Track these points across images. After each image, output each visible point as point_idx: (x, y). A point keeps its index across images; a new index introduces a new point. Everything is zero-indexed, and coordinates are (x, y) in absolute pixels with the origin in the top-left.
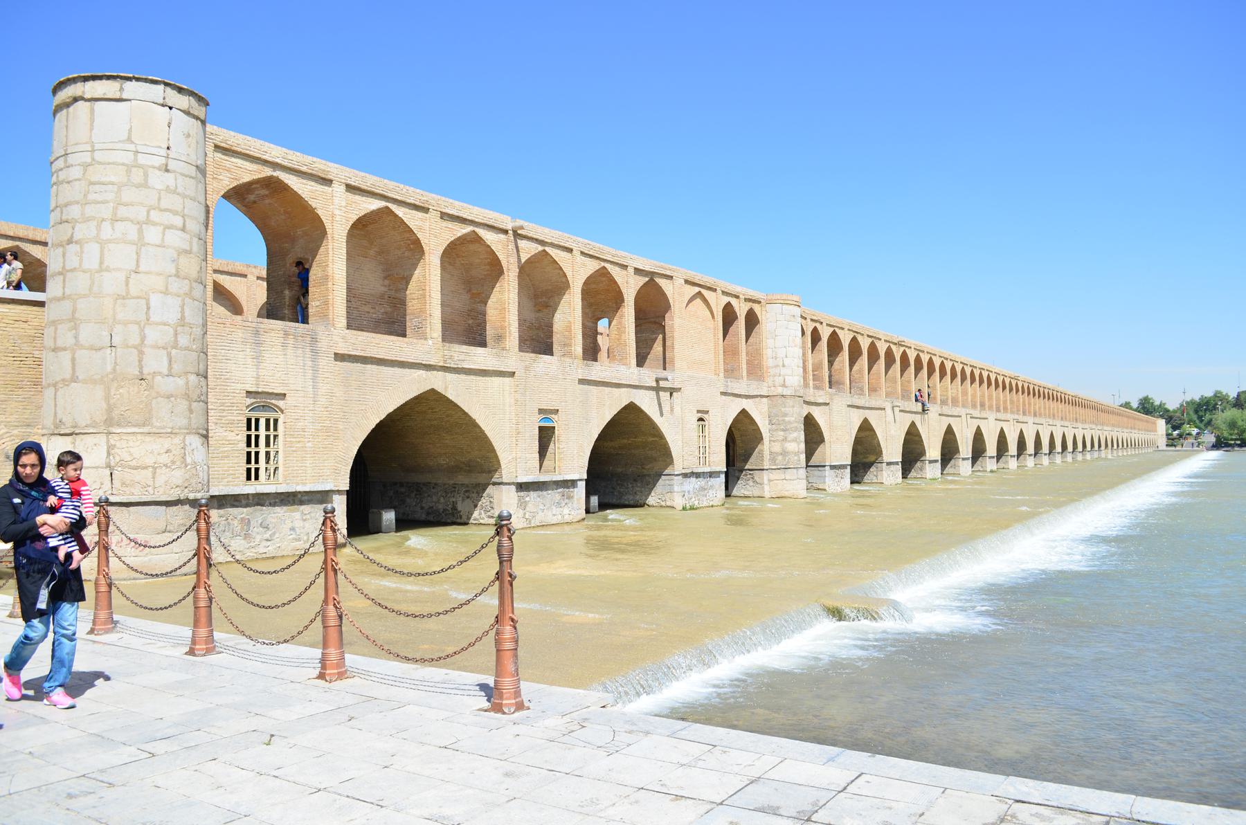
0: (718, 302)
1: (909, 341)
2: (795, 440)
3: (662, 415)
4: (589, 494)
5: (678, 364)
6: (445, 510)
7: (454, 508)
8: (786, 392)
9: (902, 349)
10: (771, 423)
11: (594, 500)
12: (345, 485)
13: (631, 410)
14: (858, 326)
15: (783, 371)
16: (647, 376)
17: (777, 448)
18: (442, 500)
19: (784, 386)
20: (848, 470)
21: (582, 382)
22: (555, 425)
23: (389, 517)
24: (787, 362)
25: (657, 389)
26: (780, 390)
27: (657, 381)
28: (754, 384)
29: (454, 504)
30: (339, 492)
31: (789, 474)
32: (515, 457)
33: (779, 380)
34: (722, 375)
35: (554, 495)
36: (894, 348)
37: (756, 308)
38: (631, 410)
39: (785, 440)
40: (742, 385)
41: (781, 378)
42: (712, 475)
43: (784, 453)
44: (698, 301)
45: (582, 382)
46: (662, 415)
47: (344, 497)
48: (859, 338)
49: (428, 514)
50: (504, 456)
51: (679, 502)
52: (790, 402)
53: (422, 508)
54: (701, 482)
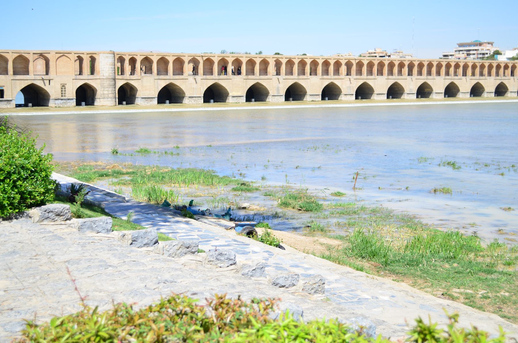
0: (74, 57)
3: (45, 85)
8: (104, 78)
17: (102, 93)
20: (156, 99)
25: (43, 80)
26: (102, 77)
31: (105, 100)
33: (102, 74)
35: (5, 103)
37: (94, 55)
43: (104, 94)
44: (64, 57)
46: (45, 85)
51: (54, 105)
52: (105, 80)
54: (65, 101)
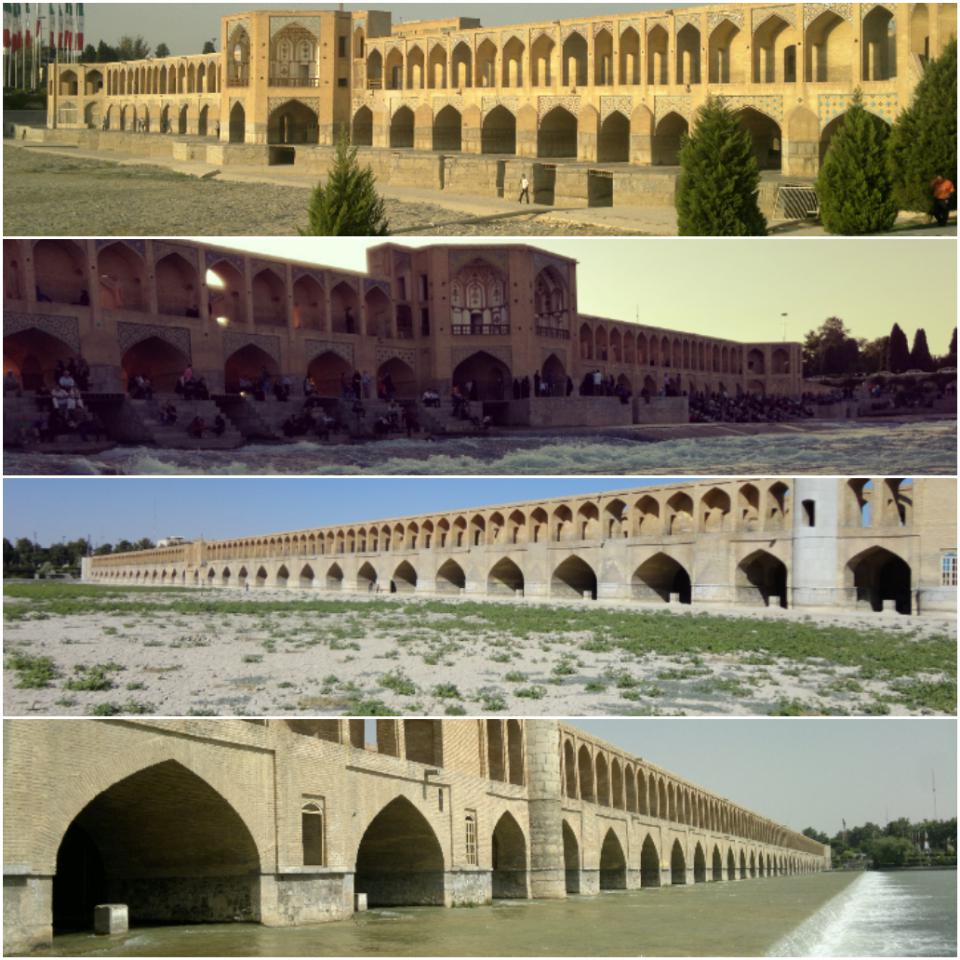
1: (646, 761)
2: (555, 843)
4: (358, 889)
5: (446, 759)
6: (194, 908)
7: (205, 905)
8: (546, 796)
9: (639, 768)
10: (531, 825)
11: (363, 898)
12: (50, 866)
13: (400, 806)
14: (604, 742)
15: (544, 776)
16: (418, 769)
17: (538, 849)
18: (190, 897)
19: (544, 790)
21: (350, 768)
22: (320, 812)
23: (120, 913)
24: (547, 767)
26: (540, 795)
27: (427, 773)
28: (517, 788)
29: (205, 901)
30: (41, 877)
32: (276, 845)
34: (487, 776)
36: (632, 766)
38: (400, 806)
39: (546, 841)
40: (505, 787)
41: (541, 784)
42: (480, 872)
45: (350, 768)
47: (49, 883)
48: (605, 754)
49: (174, 913)
50: (264, 845)
53: (167, 907)
